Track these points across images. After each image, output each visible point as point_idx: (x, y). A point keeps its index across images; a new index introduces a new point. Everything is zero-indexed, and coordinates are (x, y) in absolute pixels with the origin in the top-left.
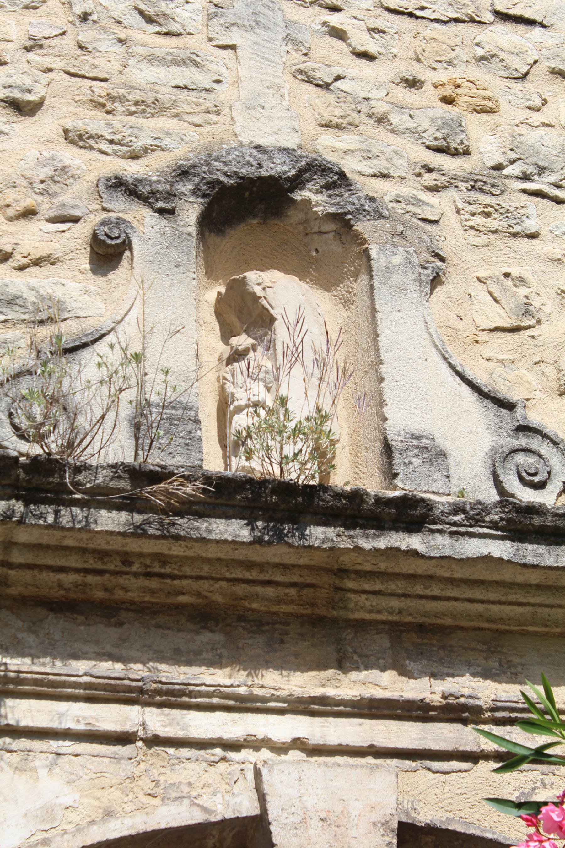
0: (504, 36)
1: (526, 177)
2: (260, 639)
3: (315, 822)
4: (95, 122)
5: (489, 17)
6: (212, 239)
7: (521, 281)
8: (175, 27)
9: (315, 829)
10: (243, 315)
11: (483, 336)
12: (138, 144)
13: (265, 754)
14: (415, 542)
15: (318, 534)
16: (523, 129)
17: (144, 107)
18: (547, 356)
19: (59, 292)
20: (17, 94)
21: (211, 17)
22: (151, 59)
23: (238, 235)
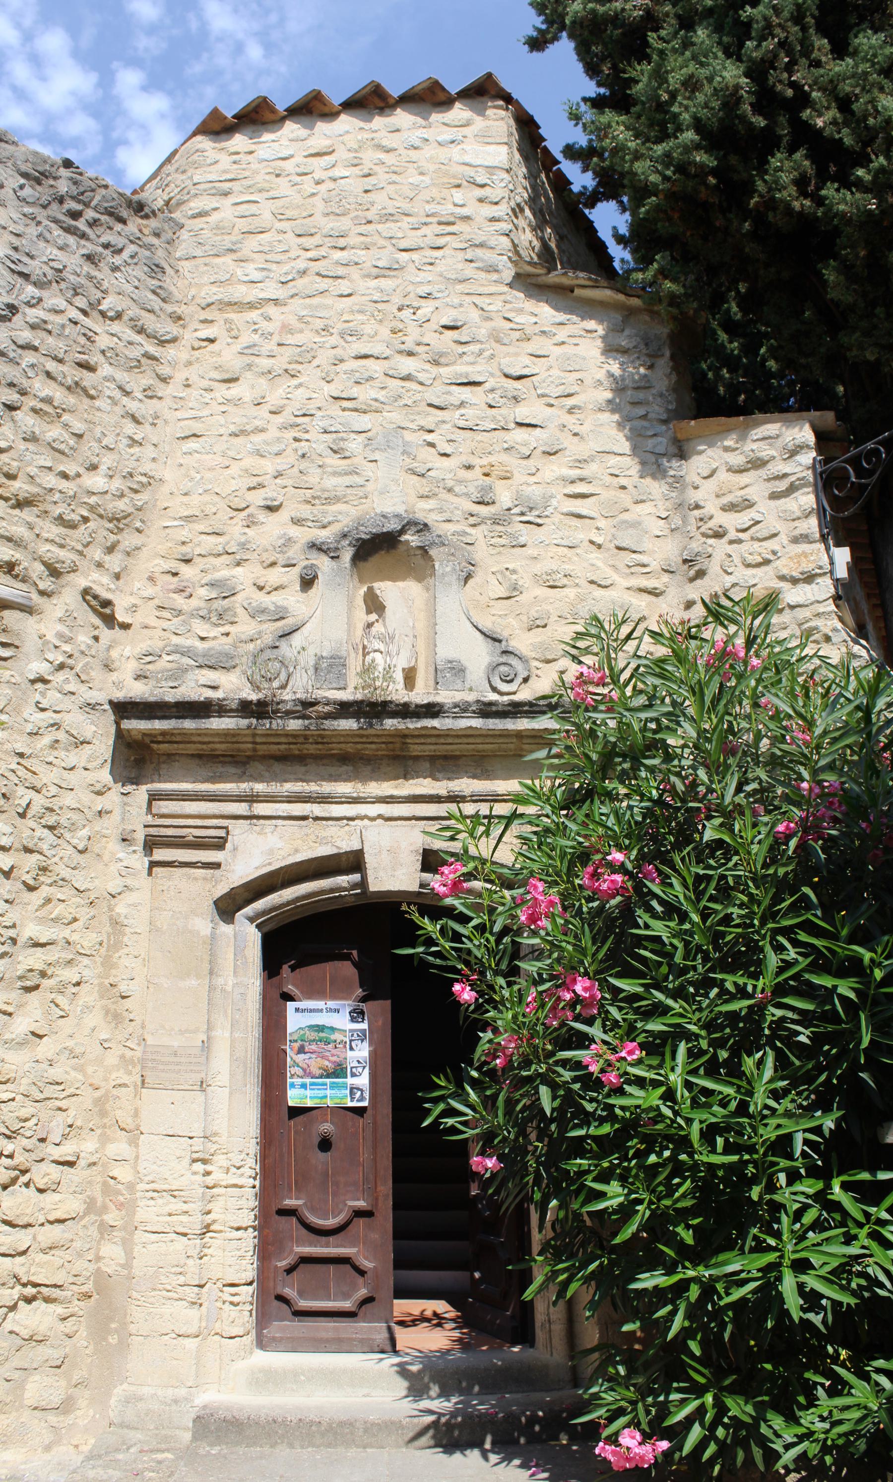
0: (520, 435)
1: (523, 514)
2: (369, 768)
3: (385, 853)
4: (305, 511)
5: (513, 425)
6: (361, 564)
7: (514, 572)
8: (347, 454)
9: (385, 854)
10: (374, 605)
11: (492, 603)
12: (326, 521)
13: (366, 822)
14: (435, 723)
15: (390, 723)
16: (524, 487)
17: (330, 500)
18: (523, 611)
19: (285, 603)
20: (269, 503)
21: (366, 446)
22: (335, 474)
23: (375, 560)
